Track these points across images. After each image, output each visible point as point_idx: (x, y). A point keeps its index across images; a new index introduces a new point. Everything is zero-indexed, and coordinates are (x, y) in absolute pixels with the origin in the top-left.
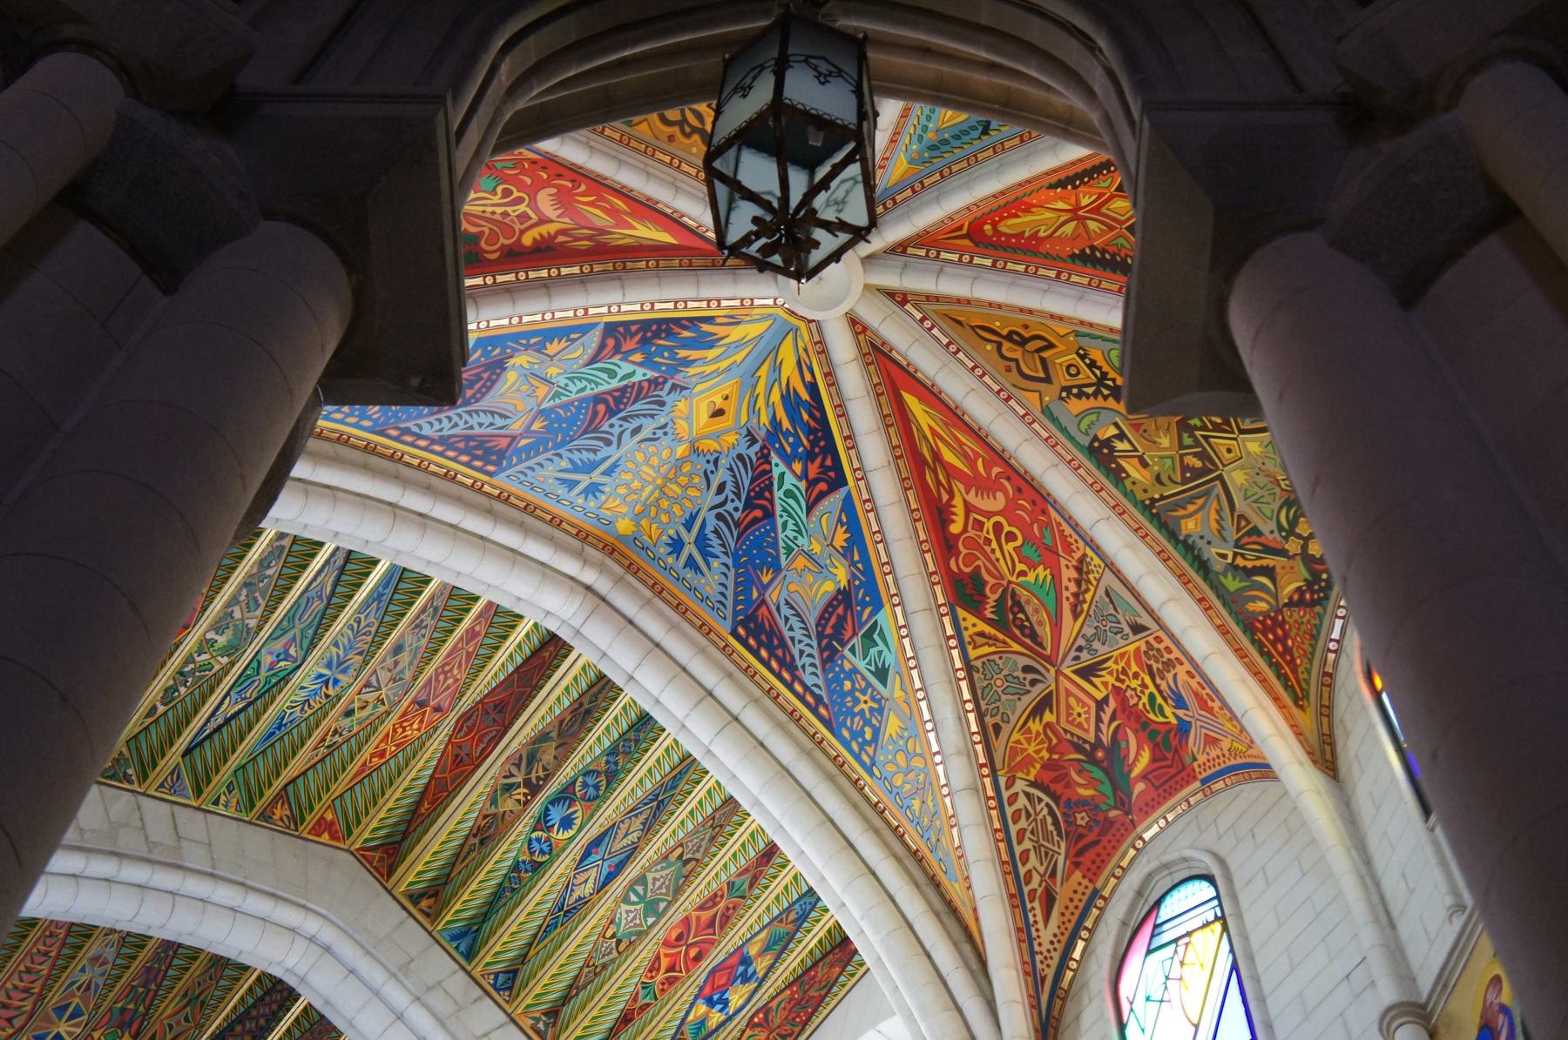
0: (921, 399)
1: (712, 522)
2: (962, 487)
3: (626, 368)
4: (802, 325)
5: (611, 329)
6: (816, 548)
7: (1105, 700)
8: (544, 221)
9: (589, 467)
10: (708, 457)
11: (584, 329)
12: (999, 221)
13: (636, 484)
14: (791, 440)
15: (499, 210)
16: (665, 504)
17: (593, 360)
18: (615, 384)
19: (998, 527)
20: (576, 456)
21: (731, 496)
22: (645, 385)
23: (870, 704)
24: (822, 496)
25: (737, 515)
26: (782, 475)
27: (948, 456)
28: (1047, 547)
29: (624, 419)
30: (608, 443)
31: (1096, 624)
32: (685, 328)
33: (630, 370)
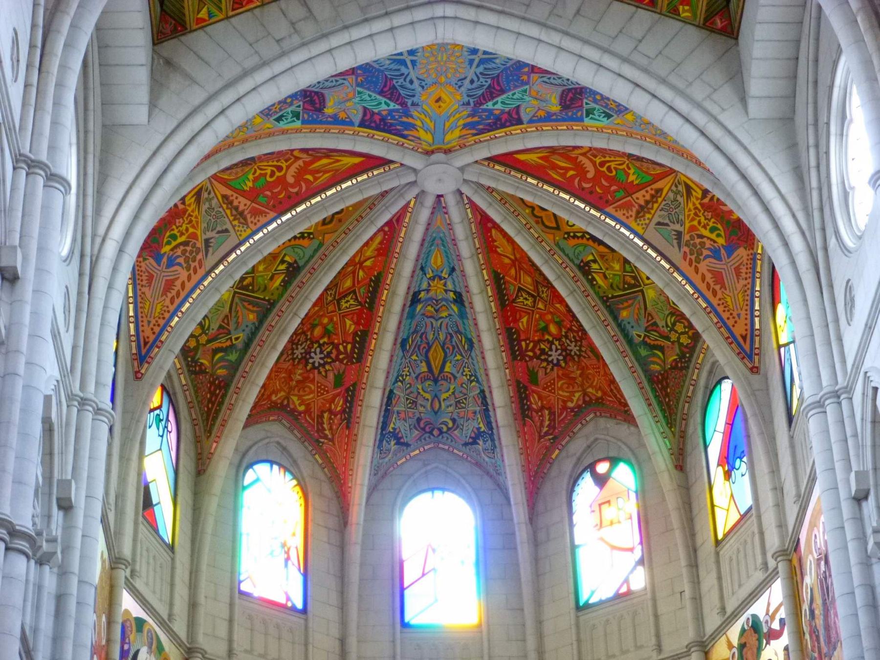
0: (356, 165)
1: (403, 70)
2: (307, 160)
3: (499, 106)
4: (430, 149)
5: (519, 122)
6: (348, 104)
7: (183, 203)
8: (584, 154)
9: (482, 62)
10: (428, 86)
11: (531, 121)
12: (384, 237)
13: (453, 59)
14: (397, 117)
15: (608, 159)
16: (432, 59)
17: (518, 107)
18: (499, 99)
19: (280, 169)
20: (494, 65)
21: (404, 83)
22: (484, 102)
23: (274, 110)
24: (365, 114)
25: (395, 81)
26: (388, 105)
27: (324, 161)
28: (258, 196)
29: (483, 86)
30: (481, 73)
31: (216, 210)
32: (482, 129)
33: (497, 105)
